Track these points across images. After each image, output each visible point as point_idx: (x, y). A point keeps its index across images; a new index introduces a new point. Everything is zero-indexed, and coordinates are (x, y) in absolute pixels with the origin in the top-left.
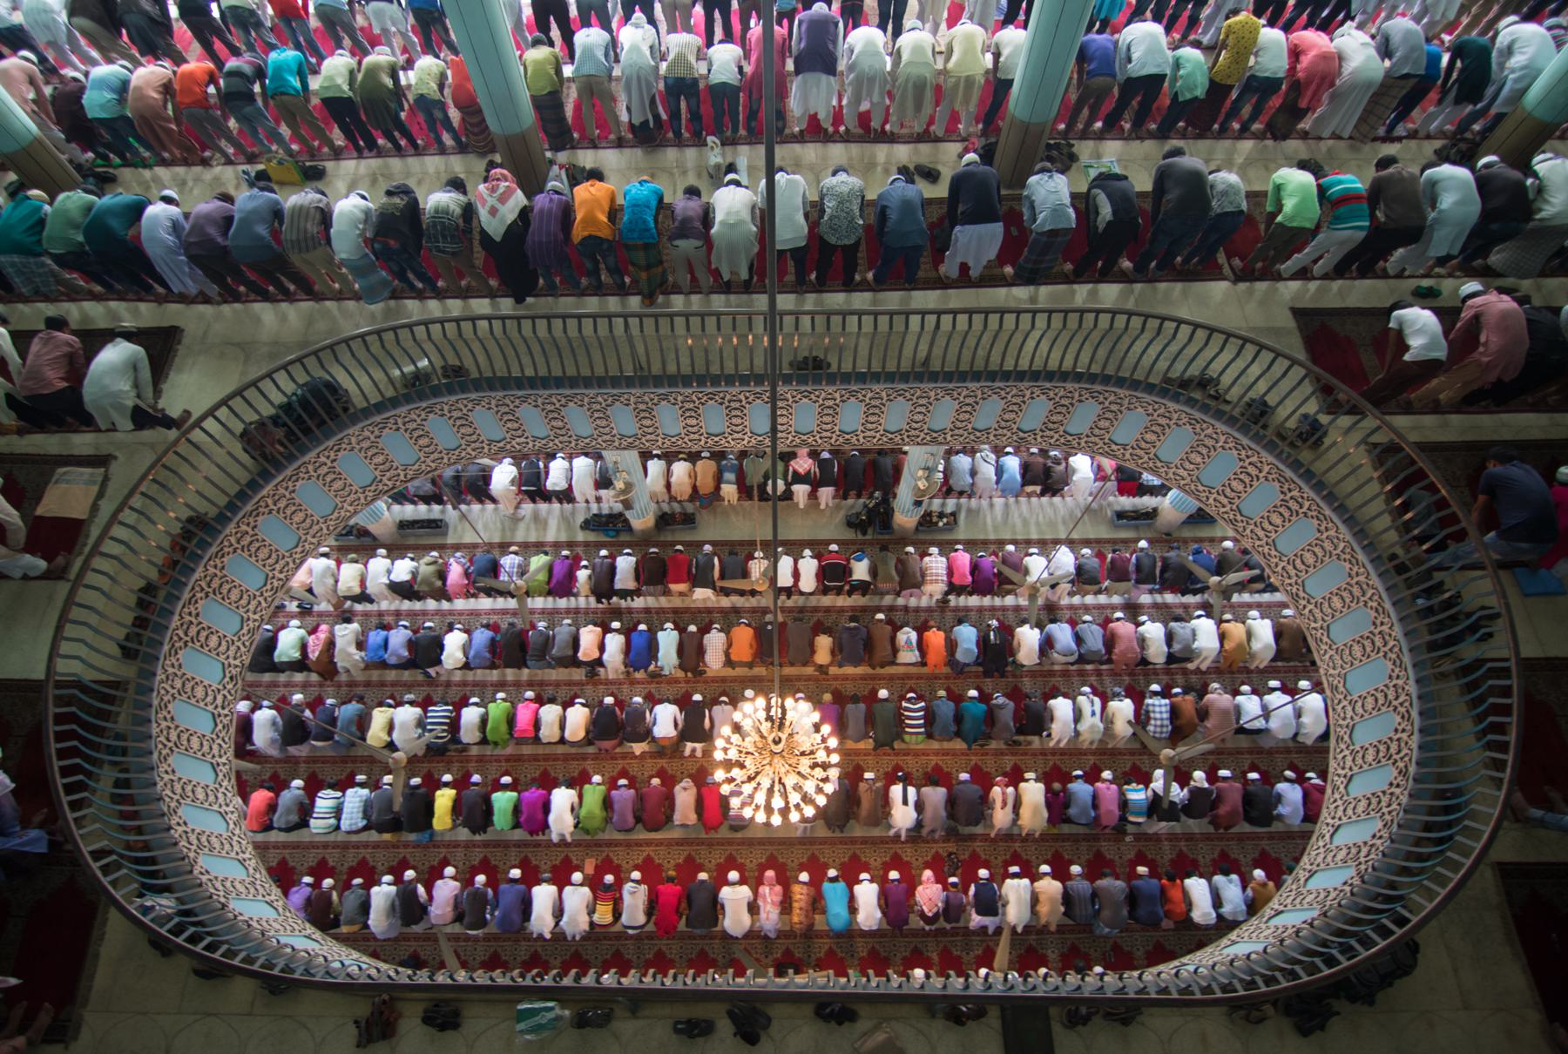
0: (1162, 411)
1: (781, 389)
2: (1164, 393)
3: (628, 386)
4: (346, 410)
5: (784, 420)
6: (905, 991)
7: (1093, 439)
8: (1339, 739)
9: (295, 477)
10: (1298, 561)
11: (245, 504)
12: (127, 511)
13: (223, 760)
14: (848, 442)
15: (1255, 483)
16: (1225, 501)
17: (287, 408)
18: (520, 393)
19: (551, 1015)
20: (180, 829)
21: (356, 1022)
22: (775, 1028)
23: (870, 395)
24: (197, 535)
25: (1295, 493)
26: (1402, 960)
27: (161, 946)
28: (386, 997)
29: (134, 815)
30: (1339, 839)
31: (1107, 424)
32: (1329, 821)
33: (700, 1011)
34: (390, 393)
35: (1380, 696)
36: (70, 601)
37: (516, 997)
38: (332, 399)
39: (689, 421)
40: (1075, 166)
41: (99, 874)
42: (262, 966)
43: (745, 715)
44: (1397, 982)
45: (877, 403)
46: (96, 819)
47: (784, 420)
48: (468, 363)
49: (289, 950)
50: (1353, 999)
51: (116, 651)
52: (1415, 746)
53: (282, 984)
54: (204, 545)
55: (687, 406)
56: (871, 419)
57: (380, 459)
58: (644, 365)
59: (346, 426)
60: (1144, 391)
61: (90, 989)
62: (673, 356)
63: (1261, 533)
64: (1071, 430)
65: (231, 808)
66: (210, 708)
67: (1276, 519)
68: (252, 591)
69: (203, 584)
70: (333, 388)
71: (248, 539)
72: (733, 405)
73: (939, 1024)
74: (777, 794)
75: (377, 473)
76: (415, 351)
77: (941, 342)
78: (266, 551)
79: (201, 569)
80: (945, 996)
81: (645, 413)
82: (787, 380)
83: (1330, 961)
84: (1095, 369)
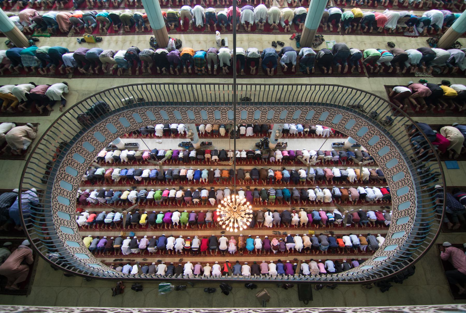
1: (237, 106)
2: (347, 109)
4: (108, 111)
5: (238, 116)
6: (271, 280)
8: (394, 209)
9: (93, 130)
10: (384, 158)
11: (78, 138)
12: (43, 140)
13: (73, 213)
14: (256, 122)
16: (364, 141)
17: (91, 110)
18: (160, 106)
19: (169, 287)
20: (60, 233)
21: (112, 289)
22: (233, 290)
24: (64, 147)
25: (384, 139)
26: (411, 271)
27: (55, 268)
28: (121, 282)
29: (46, 229)
30: (394, 237)
31: (331, 118)
32: (391, 232)
33: (211, 286)
34: (122, 106)
35: (406, 197)
36: (26, 167)
37: (158, 282)
38: (104, 108)
39: (210, 116)
40: (323, 42)
41: (36, 247)
42: (84, 273)
43: (225, 202)
44: (409, 277)
45: (265, 111)
46: (34, 230)
47: (238, 116)
48: (145, 97)
49: (92, 268)
50: (396, 282)
51: (40, 181)
52: (416, 211)
53: (90, 278)
54: (66, 150)
55: (210, 111)
56: (263, 115)
57: (119, 125)
58: (197, 99)
59: (109, 116)
60: (342, 109)
61: (34, 280)
62: (205, 96)
63: (374, 150)
66: (69, 198)
67: (379, 146)
68: (81, 164)
69: (66, 162)
70: (105, 104)
71: (79, 149)
72: (223, 111)
73: (280, 289)
74: (236, 223)
76: (129, 94)
77: (284, 93)
78: (85, 152)
79: (65, 157)
80: (282, 282)
81: (197, 113)
82: (239, 104)
83: (391, 272)
84: (328, 102)
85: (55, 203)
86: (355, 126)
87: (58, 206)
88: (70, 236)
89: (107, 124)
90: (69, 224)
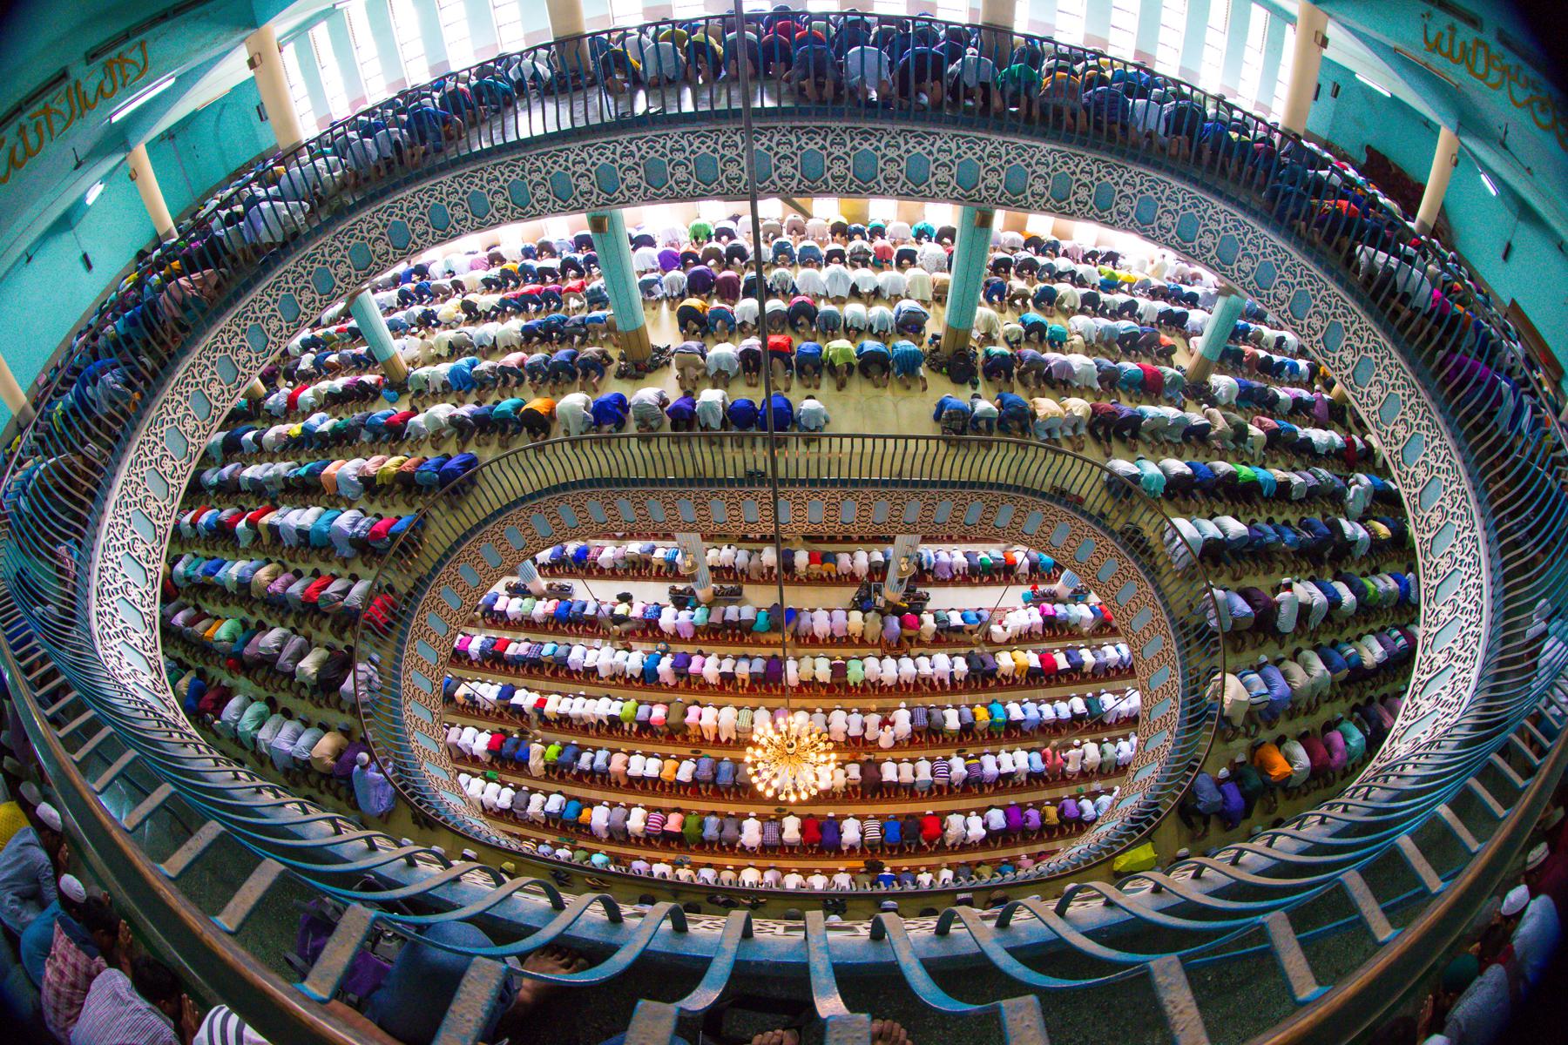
2: (1051, 498)
81: (701, 505)
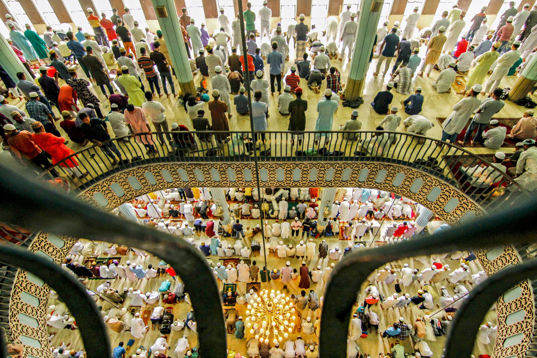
0: (410, 172)
3: (216, 161)
7: (386, 185)
9: (93, 190)
13: (45, 298)
15: (449, 199)
16: (438, 207)
18: (179, 163)
23: (303, 166)
25: (465, 201)
32: (500, 337)
47: (273, 176)
52: (533, 300)
57: (126, 187)
60: (402, 164)
64: (377, 181)
65: (42, 318)
75: (125, 192)
81: (223, 172)
85: (21, 279)
86: (424, 187)
87: (24, 285)
88: (29, 330)
89: (112, 183)
90: (34, 313)
